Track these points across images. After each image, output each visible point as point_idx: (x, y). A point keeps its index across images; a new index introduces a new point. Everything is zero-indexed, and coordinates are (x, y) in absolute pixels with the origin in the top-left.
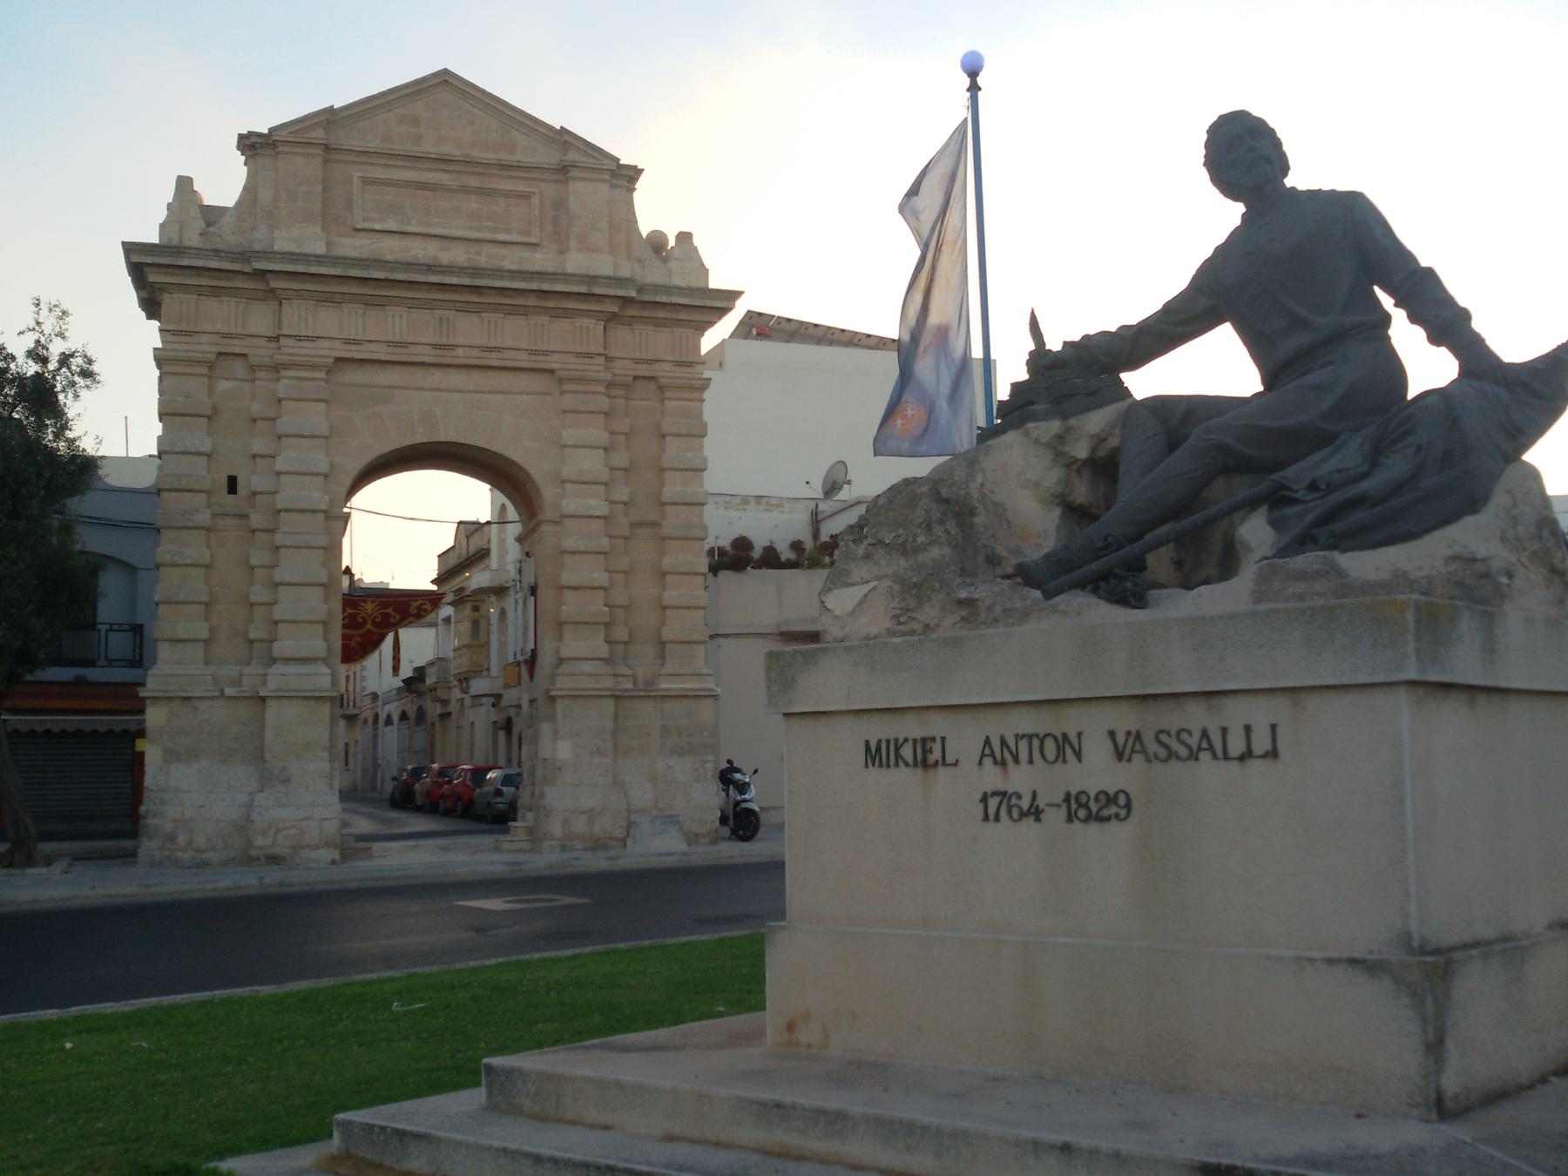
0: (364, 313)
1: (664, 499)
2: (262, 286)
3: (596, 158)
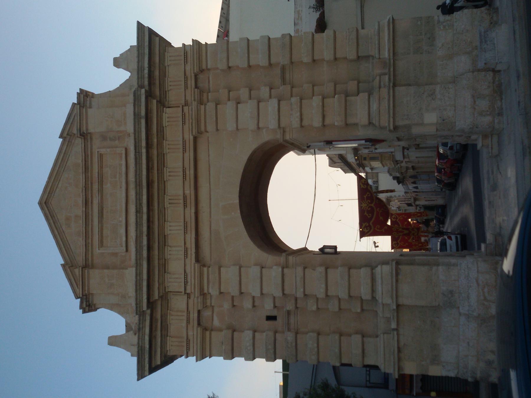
0: (170, 247)
1: (267, 64)
2: (159, 303)
3: (74, 117)
